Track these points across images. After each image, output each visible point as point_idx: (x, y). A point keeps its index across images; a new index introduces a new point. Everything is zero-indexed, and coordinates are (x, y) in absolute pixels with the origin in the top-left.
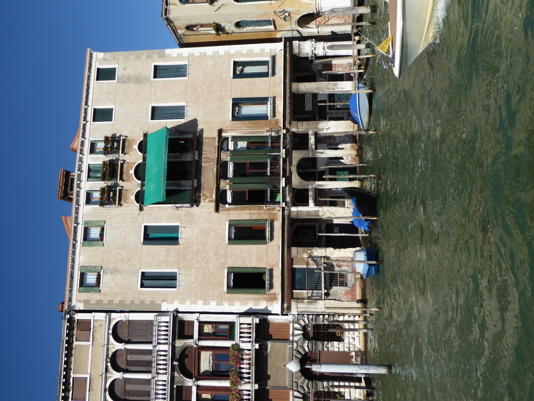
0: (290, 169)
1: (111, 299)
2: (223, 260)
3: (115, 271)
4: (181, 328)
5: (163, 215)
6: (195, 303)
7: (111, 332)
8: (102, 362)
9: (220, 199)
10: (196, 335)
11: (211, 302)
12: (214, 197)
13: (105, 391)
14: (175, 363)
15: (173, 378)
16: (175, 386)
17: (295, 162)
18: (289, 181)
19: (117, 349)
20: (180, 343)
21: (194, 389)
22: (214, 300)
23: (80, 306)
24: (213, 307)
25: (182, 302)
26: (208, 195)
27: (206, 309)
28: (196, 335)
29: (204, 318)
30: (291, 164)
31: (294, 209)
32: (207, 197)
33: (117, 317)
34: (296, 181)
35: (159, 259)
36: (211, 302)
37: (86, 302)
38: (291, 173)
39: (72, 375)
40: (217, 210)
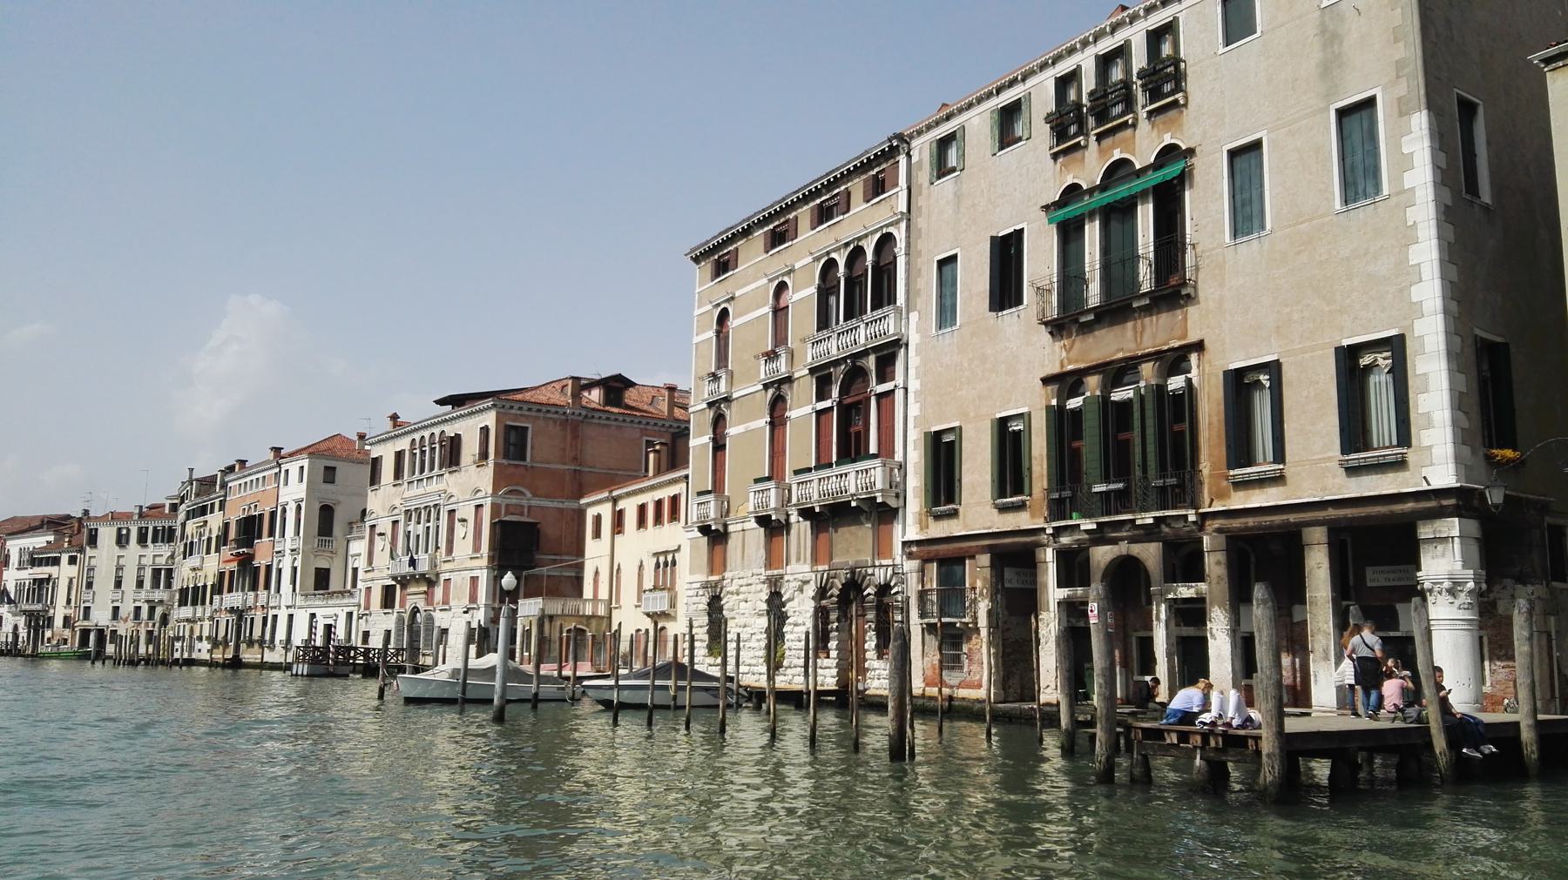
0: (1122, 539)
5: (1040, 262)
9: (1066, 382)
12: (1070, 367)
17: (1137, 549)
18: (1100, 536)
21: (827, 404)
24: (914, 410)
25: (918, 353)
26: (1073, 354)
29: (899, 394)
30: (1132, 540)
32: (1068, 352)
33: (900, 234)
34: (1102, 555)
38: (1114, 541)
40: (1046, 381)
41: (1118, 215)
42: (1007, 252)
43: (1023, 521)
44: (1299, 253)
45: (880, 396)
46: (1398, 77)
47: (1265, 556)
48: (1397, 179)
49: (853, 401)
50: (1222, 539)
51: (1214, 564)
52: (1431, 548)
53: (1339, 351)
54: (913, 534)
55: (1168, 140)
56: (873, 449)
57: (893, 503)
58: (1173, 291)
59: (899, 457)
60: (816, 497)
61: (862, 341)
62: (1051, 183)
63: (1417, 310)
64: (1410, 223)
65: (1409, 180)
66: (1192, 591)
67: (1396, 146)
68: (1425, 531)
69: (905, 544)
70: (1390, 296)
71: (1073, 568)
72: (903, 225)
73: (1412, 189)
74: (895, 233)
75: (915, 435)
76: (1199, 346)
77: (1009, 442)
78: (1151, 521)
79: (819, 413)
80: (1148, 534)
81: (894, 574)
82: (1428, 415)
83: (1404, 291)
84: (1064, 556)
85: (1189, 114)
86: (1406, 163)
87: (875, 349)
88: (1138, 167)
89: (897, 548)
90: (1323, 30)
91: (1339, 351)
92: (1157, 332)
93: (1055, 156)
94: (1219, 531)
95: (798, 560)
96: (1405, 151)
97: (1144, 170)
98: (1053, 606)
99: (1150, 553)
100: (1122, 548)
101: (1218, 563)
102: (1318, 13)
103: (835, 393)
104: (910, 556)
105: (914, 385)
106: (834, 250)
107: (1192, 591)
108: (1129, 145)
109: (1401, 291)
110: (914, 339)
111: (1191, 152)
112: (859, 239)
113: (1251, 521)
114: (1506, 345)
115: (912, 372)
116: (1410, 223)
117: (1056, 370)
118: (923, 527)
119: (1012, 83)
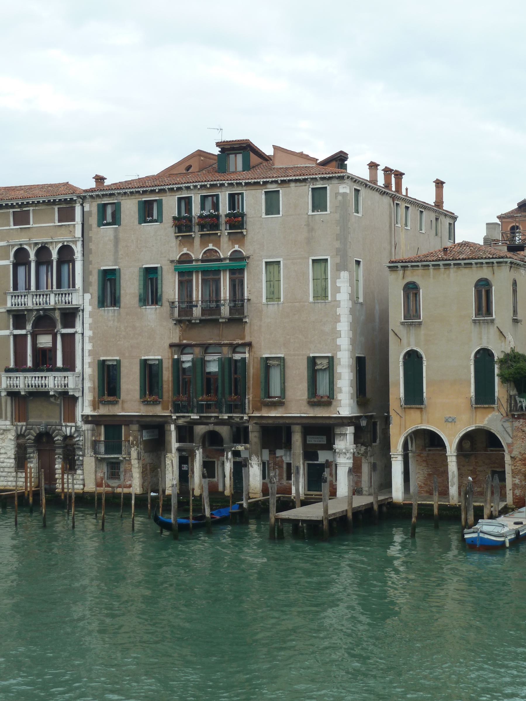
0: (211, 423)
1: (93, 239)
2: (127, 355)
3: (116, 240)
4: (70, 316)
6: (90, 329)
7: (65, 244)
11: (91, 344)
13: (21, 245)
15: (31, 310)
16: (26, 313)
17: (218, 428)
19: (52, 252)
20: (57, 315)
21: (23, 332)
22: (93, 346)
23: (87, 208)
24: (88, 346)
25: (90, 316)
27: (86, 340)
29: (78, 337)
30: (215, 424)
31: (173, 427)
34: (200, 430)
36: (91, 344)
37: (90, 212)
40: (171, 346)
41: (211, 277)
43: (158, 411)
44: (294, 314)
45: (63, 335)
46: (337, 255)
47: (276, 436)
48: (334, 296)
50: (257, 428)
51: (254, 436)
52: (339, 437)
53: (309, 358)
54: (88, 411)
55: (237, 247)
56: (59, 363)
57: (77, 395)
58: (237, 319)
59: (78, 368)
60: (22, 386)
61: (52, 303)
62: (175, 249)
63: (338, 348)
64: (338, 314)
65: (339, 297)
66: (243, 447)
67: (334, 283)
68: (338, 431)
69: (82, 416)
70: (329, 340)
71: (185, 433)
72: (79, 244)
73: (339, 301)
74: (73, 246)
75: (88, 359)
76: (249, 345)
77: (150, 372)
78: (227, 418)
79: (15, 336)
80: (222, 422)
81: (76, 430)
82: (340, 389)
83: (334, 340)
84: (179, 428)
85: (248, 240)
86: (337, 290)
87: (59, 309)
88: (222, 256)
89: (79, 418)
90: (308, 225)
91: (309, 358)
92: (229, 336)
93: (177, 237)
94: (256, 423)
96: (338, 285)
97: (225, 259)
98: (174, 450)
99: (224, 431)
100: (211, 427)
101: (255, 437)
102: (306, 216)
103: (29, 327)
105: (88, 333)
106: (26, 244)
107: (243, 447)
108: (217, 243)
109: (333, 339)
110: (88, 308)
111: (248, 257)
112: (46, 243)
113: (270, 421)
114: (364, 357)
115: (86, 326)
116: (338, 314)
117: (176, 341)
118: (95, 407)
119: (153, 192)
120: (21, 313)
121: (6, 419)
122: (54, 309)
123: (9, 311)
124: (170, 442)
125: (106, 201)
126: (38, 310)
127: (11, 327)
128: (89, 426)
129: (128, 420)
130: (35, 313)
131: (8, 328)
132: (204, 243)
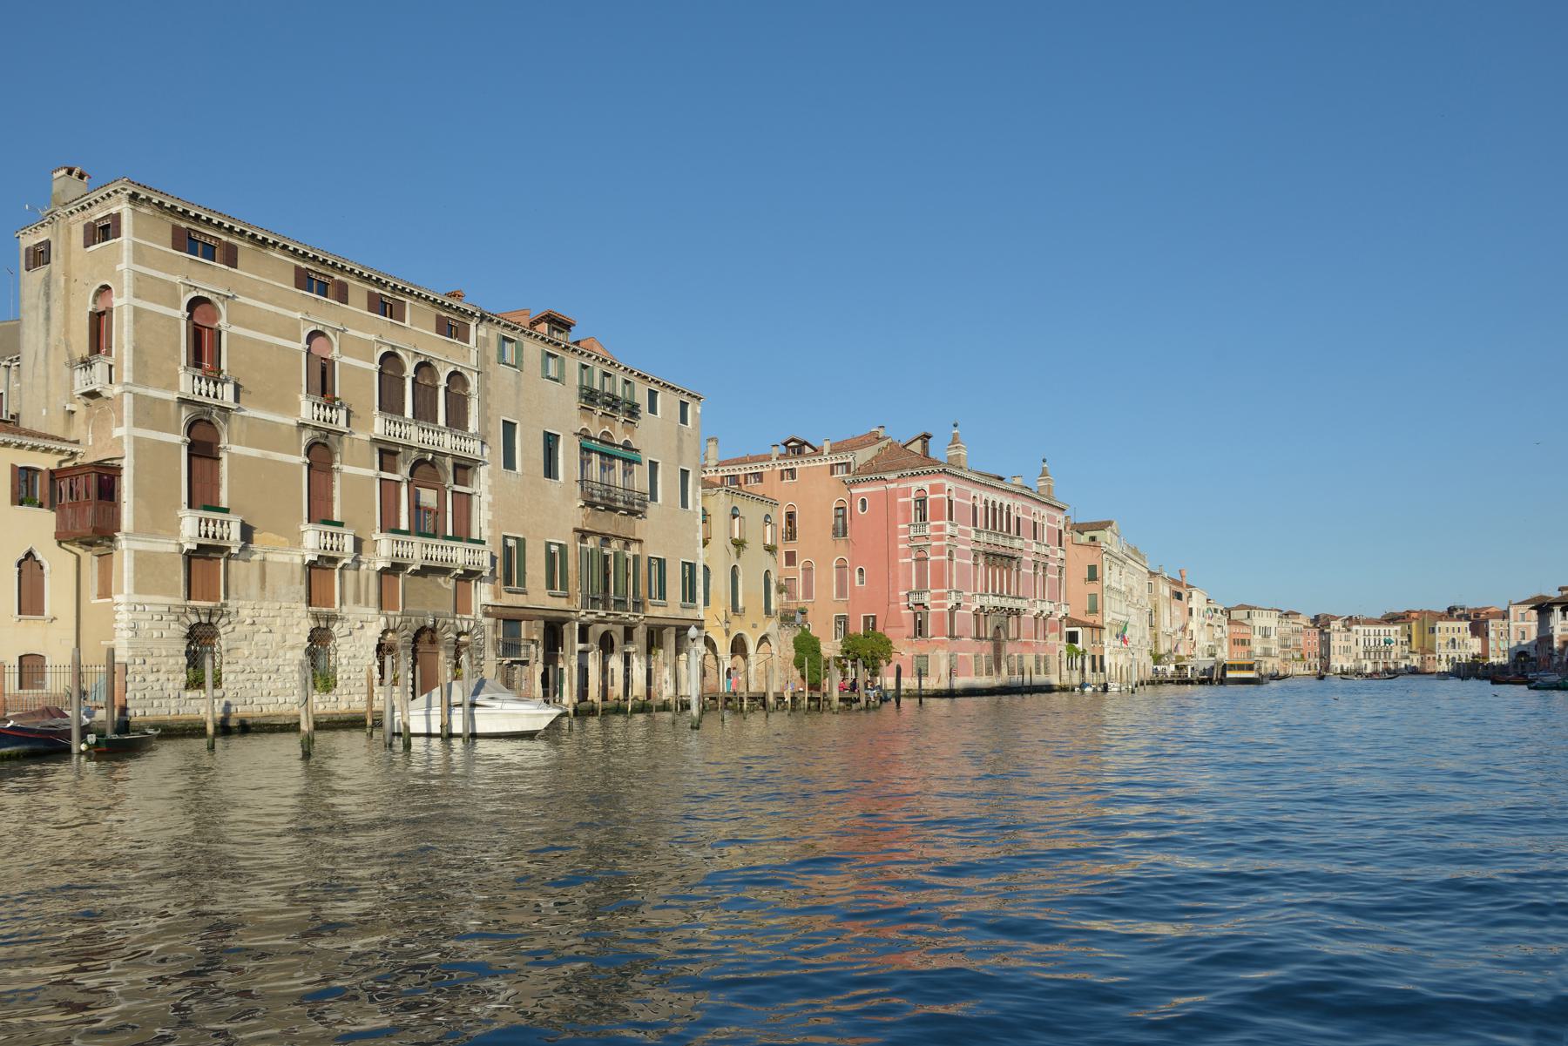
4: (464, 468)
8: (427, 352)
9: (584, 535)
10: (458, 488)
14: (430, 456)
18: (601, 621)
20: (449, 462)
25: (491, 474)
28: (458, 488)
33: (473, 380)
34: (602, 628)
35: (528, 449)
39: (408, 301)
40: (576, 530)
42: (550, 441)
49: (428, 486)
76: (640, 541)
77: (555, 561)
95: (357, 601)
104: (486, 614)
120: (393, 448)
121: (367, 605)
122: (445, 455)
123: (375, 441)
124: (572, 642)
125: (507, 333)
126: (422, 450)
127: (377, 466)
128: (491, 620)
129: (528, 614)
130: (415, 453)
131: (372, 467)
132: (602, 424)
